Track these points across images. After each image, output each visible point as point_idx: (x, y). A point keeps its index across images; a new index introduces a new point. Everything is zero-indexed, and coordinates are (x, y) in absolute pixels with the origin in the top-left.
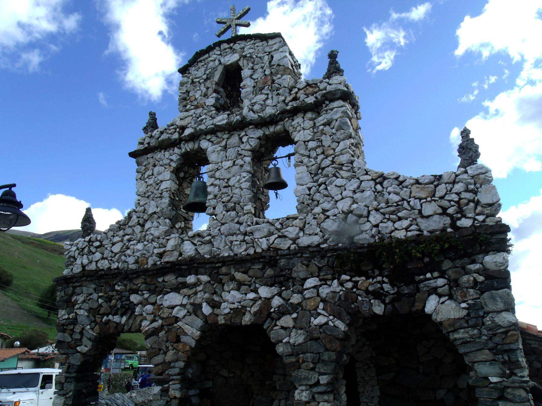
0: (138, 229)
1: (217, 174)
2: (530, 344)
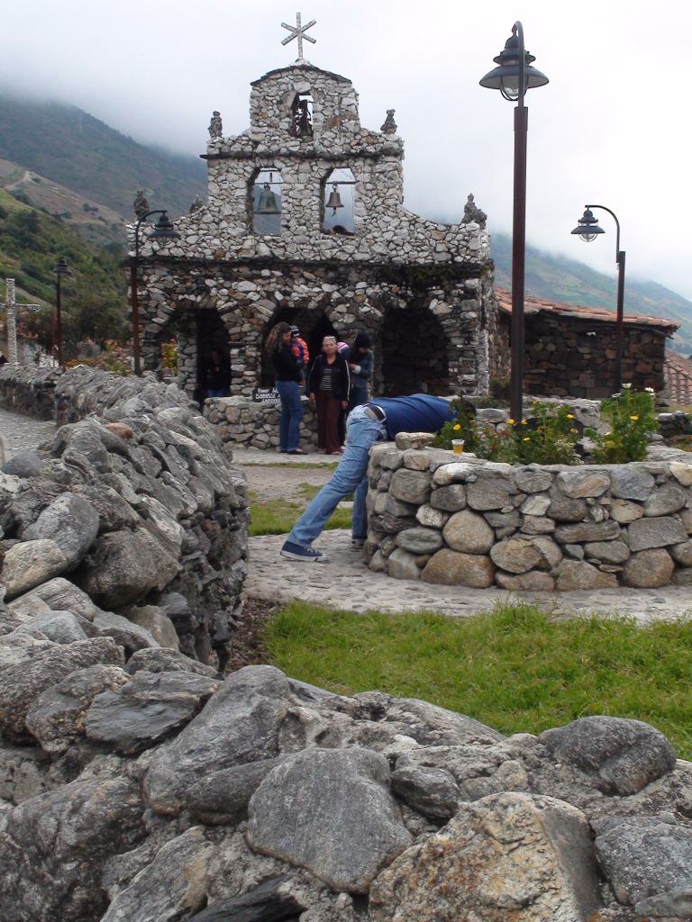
0: (213, 226)
1: (291, 193)
2: (549, 323)
